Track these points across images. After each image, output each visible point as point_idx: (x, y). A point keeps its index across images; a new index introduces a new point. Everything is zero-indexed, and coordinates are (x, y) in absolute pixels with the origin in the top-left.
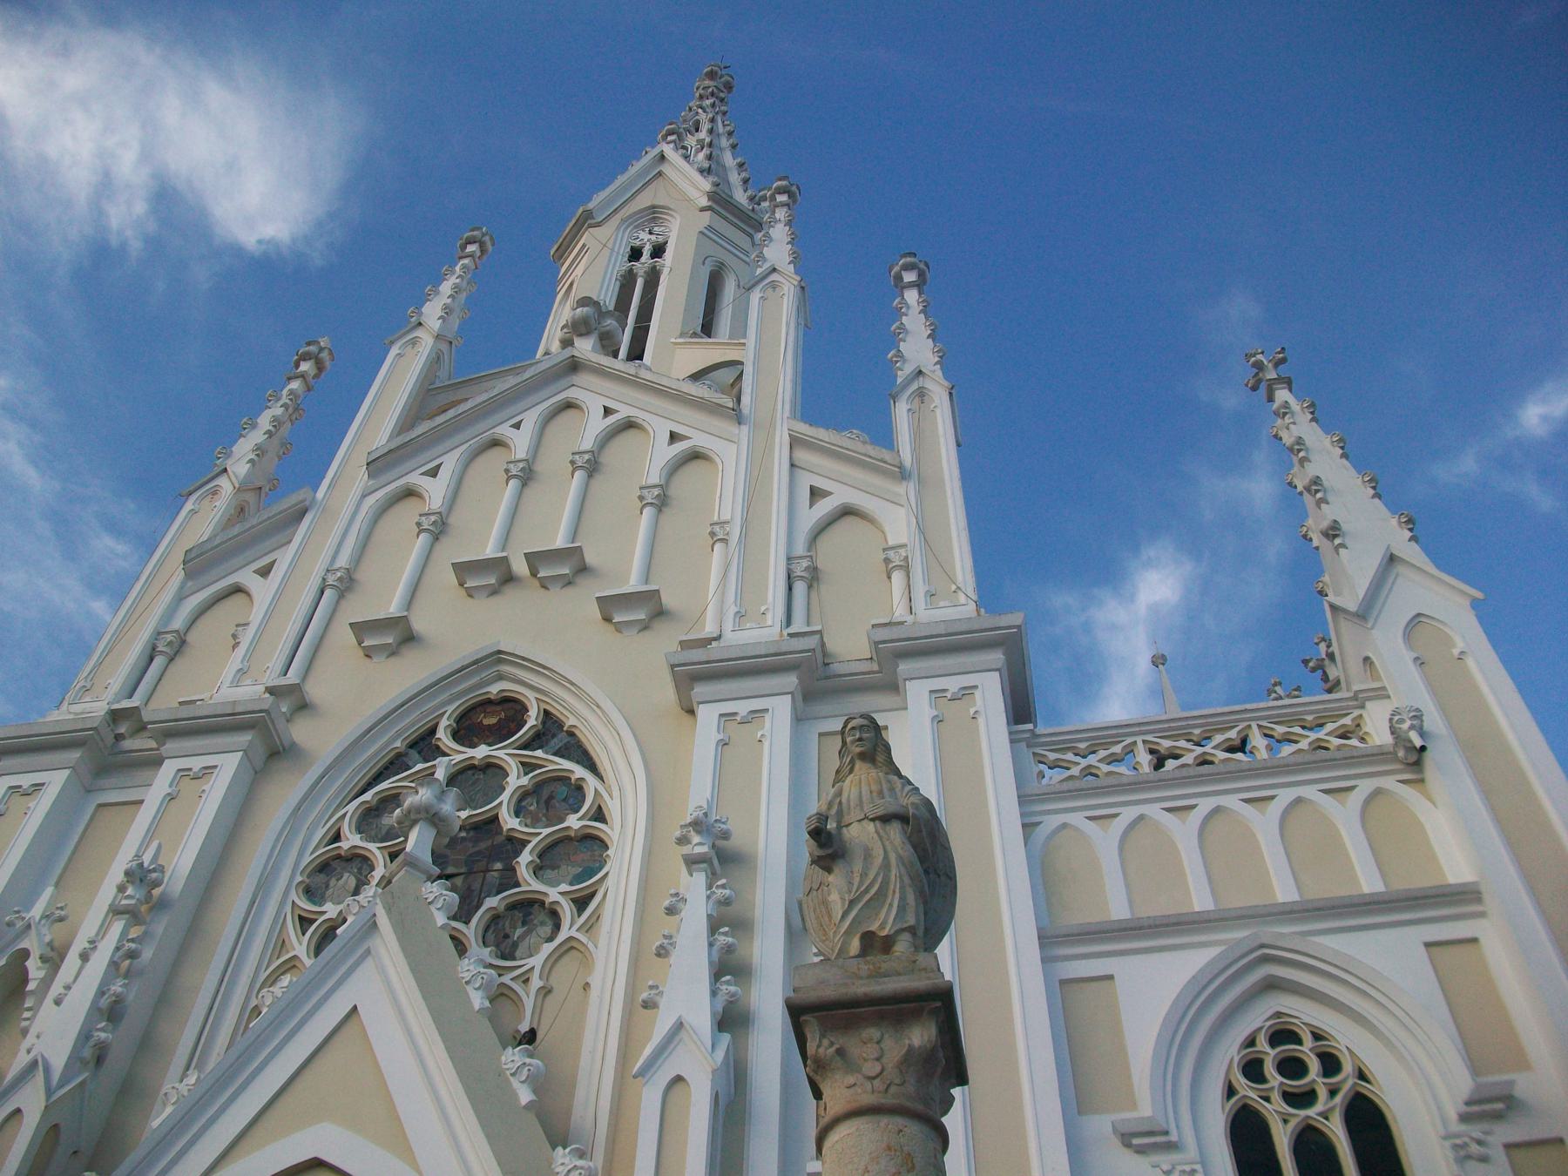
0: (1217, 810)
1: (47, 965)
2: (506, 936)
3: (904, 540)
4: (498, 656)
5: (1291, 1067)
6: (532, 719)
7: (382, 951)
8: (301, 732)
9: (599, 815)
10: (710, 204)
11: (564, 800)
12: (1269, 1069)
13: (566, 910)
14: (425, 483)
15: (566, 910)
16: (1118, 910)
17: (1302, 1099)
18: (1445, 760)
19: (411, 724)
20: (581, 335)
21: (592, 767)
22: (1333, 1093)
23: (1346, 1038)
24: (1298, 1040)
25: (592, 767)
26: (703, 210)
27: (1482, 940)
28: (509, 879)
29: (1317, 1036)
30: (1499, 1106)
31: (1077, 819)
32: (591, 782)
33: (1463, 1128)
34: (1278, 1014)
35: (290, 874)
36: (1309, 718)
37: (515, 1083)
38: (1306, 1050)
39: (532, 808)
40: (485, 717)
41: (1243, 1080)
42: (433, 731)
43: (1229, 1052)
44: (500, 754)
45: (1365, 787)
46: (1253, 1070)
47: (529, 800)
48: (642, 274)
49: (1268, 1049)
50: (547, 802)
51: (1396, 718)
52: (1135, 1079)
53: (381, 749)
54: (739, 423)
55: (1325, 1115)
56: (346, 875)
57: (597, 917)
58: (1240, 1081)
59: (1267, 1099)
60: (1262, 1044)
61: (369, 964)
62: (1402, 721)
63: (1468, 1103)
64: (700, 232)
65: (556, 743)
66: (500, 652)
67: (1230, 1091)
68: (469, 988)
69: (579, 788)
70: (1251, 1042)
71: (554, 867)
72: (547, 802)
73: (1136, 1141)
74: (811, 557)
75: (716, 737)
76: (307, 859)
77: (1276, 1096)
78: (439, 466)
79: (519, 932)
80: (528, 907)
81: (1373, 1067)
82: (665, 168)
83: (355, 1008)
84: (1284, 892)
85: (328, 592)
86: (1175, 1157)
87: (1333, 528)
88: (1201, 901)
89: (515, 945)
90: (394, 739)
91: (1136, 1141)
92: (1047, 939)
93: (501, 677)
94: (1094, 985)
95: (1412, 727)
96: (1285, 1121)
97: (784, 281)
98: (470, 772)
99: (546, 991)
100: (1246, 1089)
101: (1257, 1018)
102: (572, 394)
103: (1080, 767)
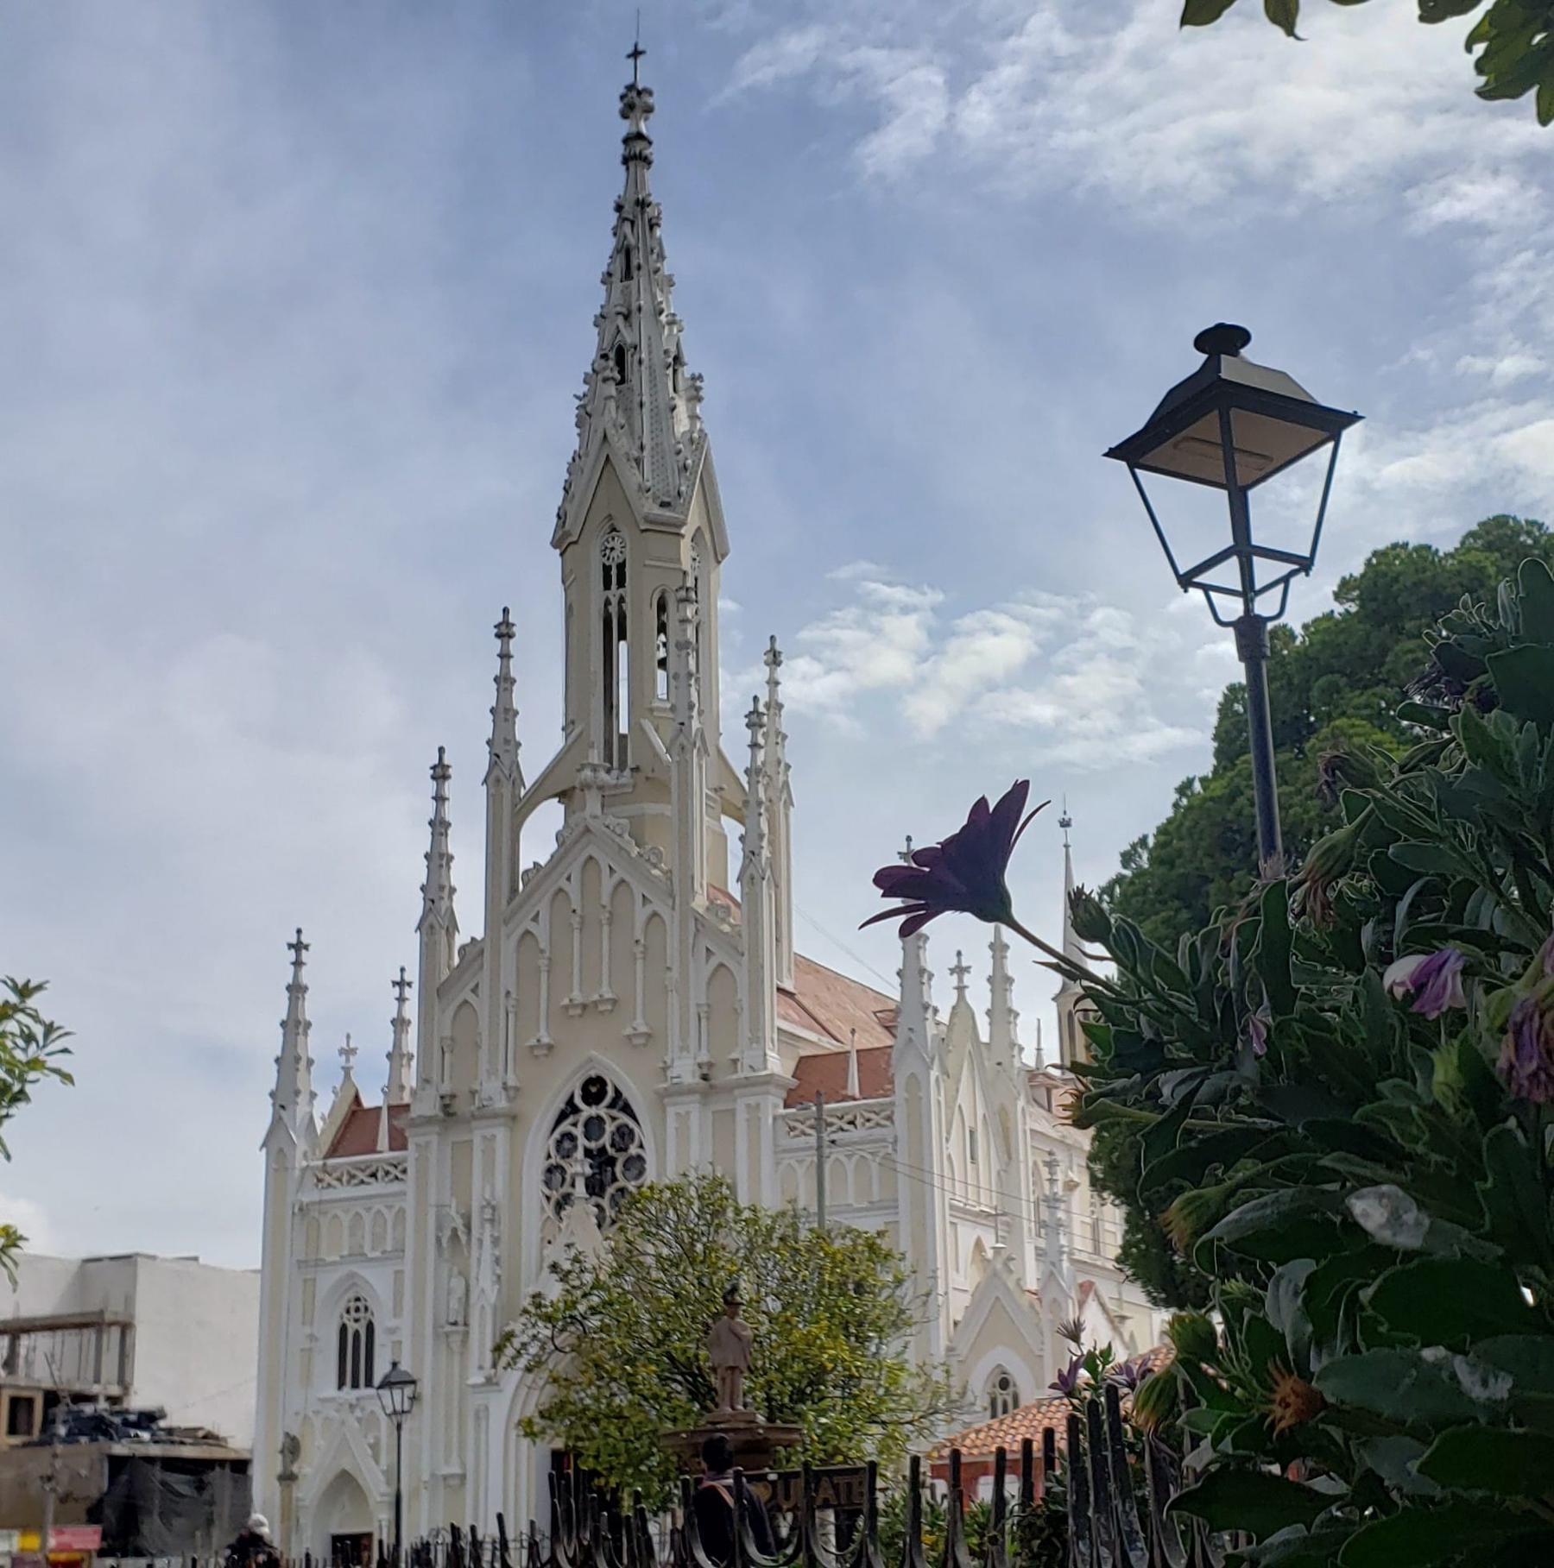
9: (641, 1146)
14: (532, 927)
19: (564, 1097)
28: (614, 1179)
32: (636, 1130)
42: (572, 1097)
69: (631, 1132)
85: (510, 1016)
93: (594, 1068)
102: (591, 850)
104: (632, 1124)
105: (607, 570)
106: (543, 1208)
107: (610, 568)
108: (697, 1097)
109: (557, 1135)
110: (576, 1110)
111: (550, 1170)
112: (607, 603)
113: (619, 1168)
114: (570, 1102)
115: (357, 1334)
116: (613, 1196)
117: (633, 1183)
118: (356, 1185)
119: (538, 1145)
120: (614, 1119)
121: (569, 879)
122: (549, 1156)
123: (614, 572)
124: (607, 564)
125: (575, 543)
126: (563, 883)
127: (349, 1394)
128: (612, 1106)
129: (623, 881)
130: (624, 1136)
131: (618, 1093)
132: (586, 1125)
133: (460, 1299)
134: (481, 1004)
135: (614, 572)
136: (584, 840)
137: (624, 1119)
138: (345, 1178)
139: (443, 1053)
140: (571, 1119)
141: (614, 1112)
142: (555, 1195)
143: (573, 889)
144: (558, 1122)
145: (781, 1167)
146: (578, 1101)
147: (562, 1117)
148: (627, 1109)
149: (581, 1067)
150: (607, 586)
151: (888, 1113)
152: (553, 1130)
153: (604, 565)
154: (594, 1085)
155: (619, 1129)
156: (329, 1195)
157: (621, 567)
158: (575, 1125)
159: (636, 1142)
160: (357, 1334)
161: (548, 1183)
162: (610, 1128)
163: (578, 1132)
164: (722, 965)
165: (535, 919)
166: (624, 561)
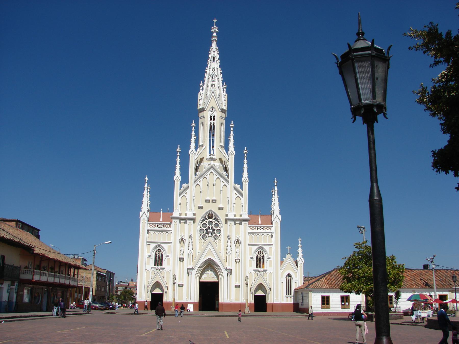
6: (214, 217)
9: (220, 228)
12: (259, 253)
13: (219, 236)
17: (260, 255)
19: (204, 216)
28: (214, 233)
32: (219, 225)
35: (199, 231)
38: (261, 252)
43: (257, 252)
44: (212, 220)
57: (221, 237)
58: (258, 254)
65: (216, 219)
78: (200, 181)
104: (218, 224)
105: (211, 117)
106: (200, 237)
107: (211, 117)
109: (202, 223)
110: (206, 219)
111: (201, 230)
112: (211, 123)
113: (215, 231)
114: (205, 217)
115: (159, 255)
116: (214, 236)
119: (198, 225)
120: (214, 222)
121: (207, 175)
122: (201, 227)
123: (212, 117)
124: (211, 116)
125: (206, 110)
126: (206, 176)
127: (157, 267)
130: (217, 225)
131: (215, 217)
135: (212, 117)
136: (210, 169)
137: (217, 222)
140: (206, 221)
141: (215, 221)
142: (202, 234)
144: (203, 221)
145: (249, 235)
146: (207, 217)
147: (203, 220)
148: (217, 220)
150: (211, 119)
152: (202, 223)
153: (210, 116)
155: (215, 224)
156: (153, 228)
157: (214, 117)
158: (206, 222)
159: (219, 227)
160: (159, 255)
162: (214, 223)
163: (207, 223)
164: (238, 197)
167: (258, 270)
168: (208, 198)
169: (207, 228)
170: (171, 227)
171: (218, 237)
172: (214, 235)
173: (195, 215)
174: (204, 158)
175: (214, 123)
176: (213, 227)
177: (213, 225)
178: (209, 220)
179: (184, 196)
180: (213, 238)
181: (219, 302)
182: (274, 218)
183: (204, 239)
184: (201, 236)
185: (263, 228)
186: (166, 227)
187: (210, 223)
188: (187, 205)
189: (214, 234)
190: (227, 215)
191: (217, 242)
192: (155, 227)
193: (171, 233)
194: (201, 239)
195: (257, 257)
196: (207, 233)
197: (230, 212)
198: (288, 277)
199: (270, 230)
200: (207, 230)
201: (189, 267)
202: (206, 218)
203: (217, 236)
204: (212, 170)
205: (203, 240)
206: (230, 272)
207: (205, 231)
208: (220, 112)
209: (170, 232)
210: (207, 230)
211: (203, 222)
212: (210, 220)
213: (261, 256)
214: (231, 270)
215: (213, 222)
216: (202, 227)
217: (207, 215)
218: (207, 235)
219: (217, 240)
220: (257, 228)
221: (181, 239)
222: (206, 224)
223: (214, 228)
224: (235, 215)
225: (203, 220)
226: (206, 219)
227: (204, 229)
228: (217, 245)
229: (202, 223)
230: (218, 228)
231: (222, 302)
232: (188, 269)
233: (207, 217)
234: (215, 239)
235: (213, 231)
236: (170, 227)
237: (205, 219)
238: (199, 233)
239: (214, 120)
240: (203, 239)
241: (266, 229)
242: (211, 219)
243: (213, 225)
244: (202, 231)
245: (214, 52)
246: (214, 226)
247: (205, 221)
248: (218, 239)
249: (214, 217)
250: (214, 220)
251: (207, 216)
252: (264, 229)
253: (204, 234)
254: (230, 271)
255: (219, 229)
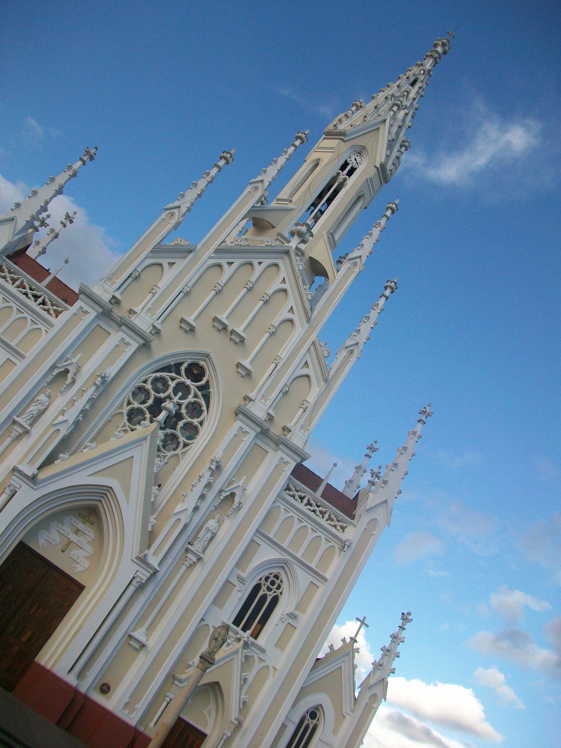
0: (306, 526)
1: (72, 380)
2: (166, 441)
3: (310, 402)
4: (208, 356)
5: (273, 583)
6: (203, 382)
7: (145, 445)
8: (155, 344)
9: (201, 423)
10: (378, 166)
11: (198, 412)
12: (269, 580)
13: (181, 445)
14: (225, 266)
15: (181, 445)
16: (271, 536)
17: (269, 589)
18: (349, 553)
19: (178, 359)
20: (298, 235)
21: (208, 407)
22: (275, 592)
23: (285, 586)
24: (278, 580)
25: (208, 407)
26: (376, 167)
27: (319, 588)
28: (174, 427)
29: (281, 581)
30: (293, 617)
31: (282, 507)
32: (205, 413)
33: (285, 615)
34: (279, 573)
35: (132, 388)
36: (340, 518)
37: (152, 496)
38: (278, 582)
39: (190, 408)
40: (195, 369)
41: (264, 579)
42: (182, 364)
43: (266, 573)
44: (192, 386)
45: (332, 544)
46: (267, 578)
47: (190, 405)
48: (339, 182)
49: (272, 577)
50: (194, 409)
51: (347, 541)
52: (249, 567)
53: (168, 362)
54: (308, 322)
55: (270, 595)
56: (143, 395)
58: (263, 579)
59: (264, 585)
60: (272, 576)
61: (140, 447)
62: (347, 542)
63: (289, 613)
64: (367, 179)
65: (205, 392)
66: (209, 355)
67: (260, 580)
68: (155, 465)
69: (201, 412)
70: (271, 574)
71: (185, 430)
72: (194, 409)
73: (239, 579)
74: (289, 388)
75: (235, 432)
76: (137, 384)
77: (266, 586)
78: (232, 263)
79: (169, 442)
80: (174, 437)
81: (283, 594)
82: (381, 127)
83: (133, 456)
84: (299, 555)
86: (243, 586)
87: (386, 482)
88: (285, 545)
89: (167, 445)
90: (172, 361)
91: (239, 579)
92: (257, 531)
93: (205, 361)
94: (257, 544)
95: (347, 545)
96: (264, 591)
97: (359, 267)
98: (183, 385)
99: (167, 463)
100: (263, 582)
101: (275, 571)
102: (280, 262)
103: (293, 493)
104: (204, 408)
105: (346, 164)
106: (121, 406)
107: (348, 165)
108: (259, 430)
109: (158, 375)
110: (178, 373)
111: (141, 389)
112: (338, 174)
113: (181, 424)
117: (184, 439)
118: (21, 292)
121: (260, 263)
122: (145, 382)
123: (349, 168)
124: (349, 161)
126: (255, 262)
128: (200, 388)
129: (285, 291)
132: (177, 384)
133: (40, 410)
134: (169, 274)
135: (349, 168)
136: (281, 255)
137: (203, 402)
138: (18, 283)
139: (129, 277)
140: (173, 374)
141: (200, 393)
142: (136, 405)
143: (259, 270)
146: (183, 368)
147: (167, 369)
148: (207, 398)
149: (197, 354)
150: (343, 168)
151: (345, 525)
152: (157, 371)
154: (197, 369)
155: (195, 403)
157: (353, 170)
158: (173, 379)
159: (200, 419)
161: (134, 394)
162: (191, 398)
163: (172, 384)
164: (308, 376)
165: (230, 264)
166: (356, 169)
167: (237, 633)
168: (223, 317)
169: (162, 395)
170: (57, 317)
171: (177, 447)
172: (169, 431)
173: (157, 332)
174: (274, 227)
175: (345, 180)
176: (183, 407)
177: (186, 402)
178: (183, 380)
179: (161, 265)
180: (161, 434)
181: (36, 659)
182: (373, 505)
183: (133, 422)
184: (130, 406)
185: (324, 510)
186: (41, 306)
187: (182, 388)
188: (151, 295)
189: (171, 428)
190: (247, 399)
191: (164, 457)
192: (11, 282)
193: (44, 332)
194: (121, 413)
195: (257, 588)
196: (155, 409)
197: (261, 399)
198: (308, 717)
199: (341, 530)
200: (159, 402)
201: (21, 467)
202: (180, 371)
203: (175, 442)
204: (280, 262)
205: (127, 423)
206: (145, 578)
207: (150, 402)
208: (376, 170)
209: (43, 329)
210: (159, 402)
211: (163, 374)
212: (188, 382)
213: (269, 593)
214: (155, 572)
215: (192, 394)
216: (149, 381)
217: (189, 361)
218: (148, 415)
219: (169, 454)
220: (308, 501)
221: (62, 370)
222: (168, 386)
223: (183, 411)
224: (271, 418)
225: (167, 369)
226: (178, 373)
227: (153, 393)
228: (160, 463)
229: (158, 375)
230: (195, 421)
231: (49, 667)
232: (15, 469)
233: (183, 368)
234: (164, 447)
235: (174, 419)
236: (54, 315)
237: (173, 369)
238: (130, 394)
239: (350, 173)
240: (130, 420)
241: (329, 522)
242: (192, 381)
243: (186, 402)
244: (142, 397)
245: (422, 72)
246: (187, 407)
247: (171, 372)
248: (173, 453)
249: (203, 382)
250: (199, 390)
251: (185, 365)
252: (326, 516)
253: (142, 406)
254: (148, 575)
255: (196, 428)
